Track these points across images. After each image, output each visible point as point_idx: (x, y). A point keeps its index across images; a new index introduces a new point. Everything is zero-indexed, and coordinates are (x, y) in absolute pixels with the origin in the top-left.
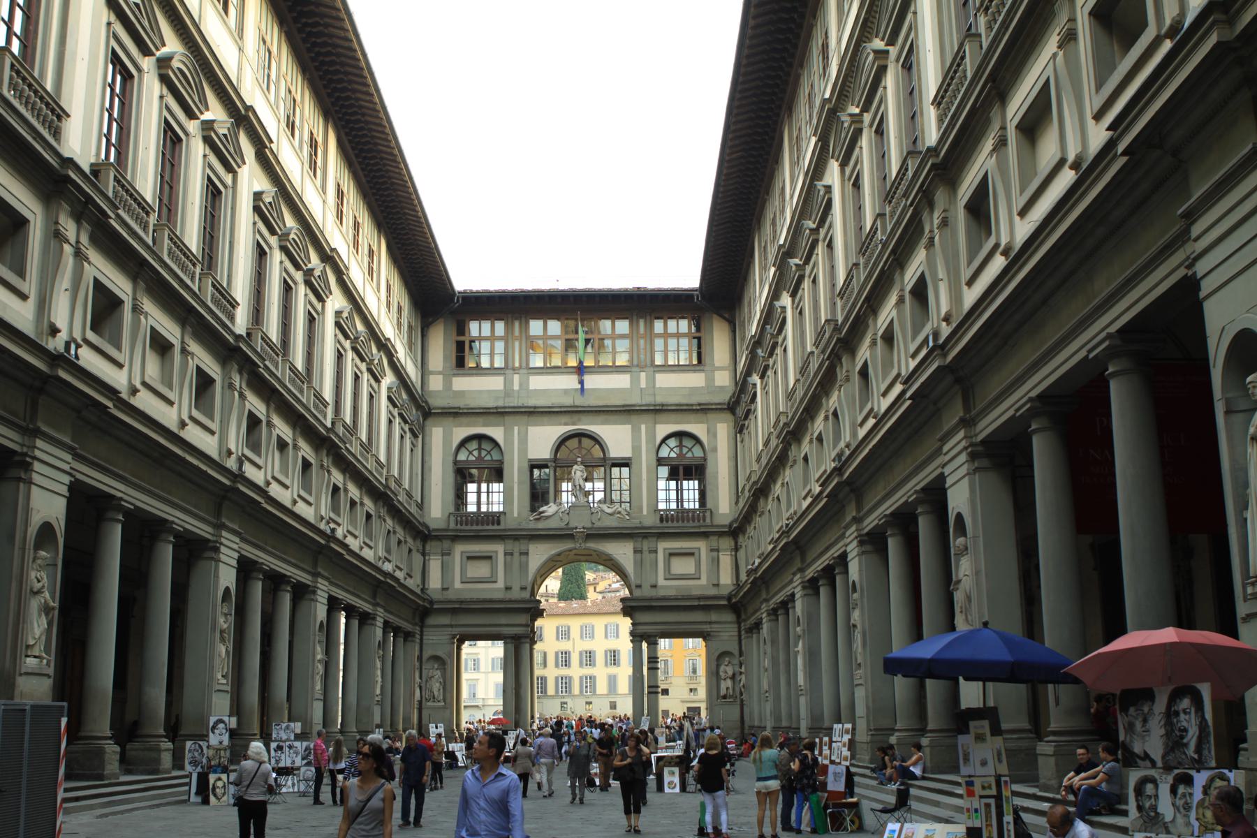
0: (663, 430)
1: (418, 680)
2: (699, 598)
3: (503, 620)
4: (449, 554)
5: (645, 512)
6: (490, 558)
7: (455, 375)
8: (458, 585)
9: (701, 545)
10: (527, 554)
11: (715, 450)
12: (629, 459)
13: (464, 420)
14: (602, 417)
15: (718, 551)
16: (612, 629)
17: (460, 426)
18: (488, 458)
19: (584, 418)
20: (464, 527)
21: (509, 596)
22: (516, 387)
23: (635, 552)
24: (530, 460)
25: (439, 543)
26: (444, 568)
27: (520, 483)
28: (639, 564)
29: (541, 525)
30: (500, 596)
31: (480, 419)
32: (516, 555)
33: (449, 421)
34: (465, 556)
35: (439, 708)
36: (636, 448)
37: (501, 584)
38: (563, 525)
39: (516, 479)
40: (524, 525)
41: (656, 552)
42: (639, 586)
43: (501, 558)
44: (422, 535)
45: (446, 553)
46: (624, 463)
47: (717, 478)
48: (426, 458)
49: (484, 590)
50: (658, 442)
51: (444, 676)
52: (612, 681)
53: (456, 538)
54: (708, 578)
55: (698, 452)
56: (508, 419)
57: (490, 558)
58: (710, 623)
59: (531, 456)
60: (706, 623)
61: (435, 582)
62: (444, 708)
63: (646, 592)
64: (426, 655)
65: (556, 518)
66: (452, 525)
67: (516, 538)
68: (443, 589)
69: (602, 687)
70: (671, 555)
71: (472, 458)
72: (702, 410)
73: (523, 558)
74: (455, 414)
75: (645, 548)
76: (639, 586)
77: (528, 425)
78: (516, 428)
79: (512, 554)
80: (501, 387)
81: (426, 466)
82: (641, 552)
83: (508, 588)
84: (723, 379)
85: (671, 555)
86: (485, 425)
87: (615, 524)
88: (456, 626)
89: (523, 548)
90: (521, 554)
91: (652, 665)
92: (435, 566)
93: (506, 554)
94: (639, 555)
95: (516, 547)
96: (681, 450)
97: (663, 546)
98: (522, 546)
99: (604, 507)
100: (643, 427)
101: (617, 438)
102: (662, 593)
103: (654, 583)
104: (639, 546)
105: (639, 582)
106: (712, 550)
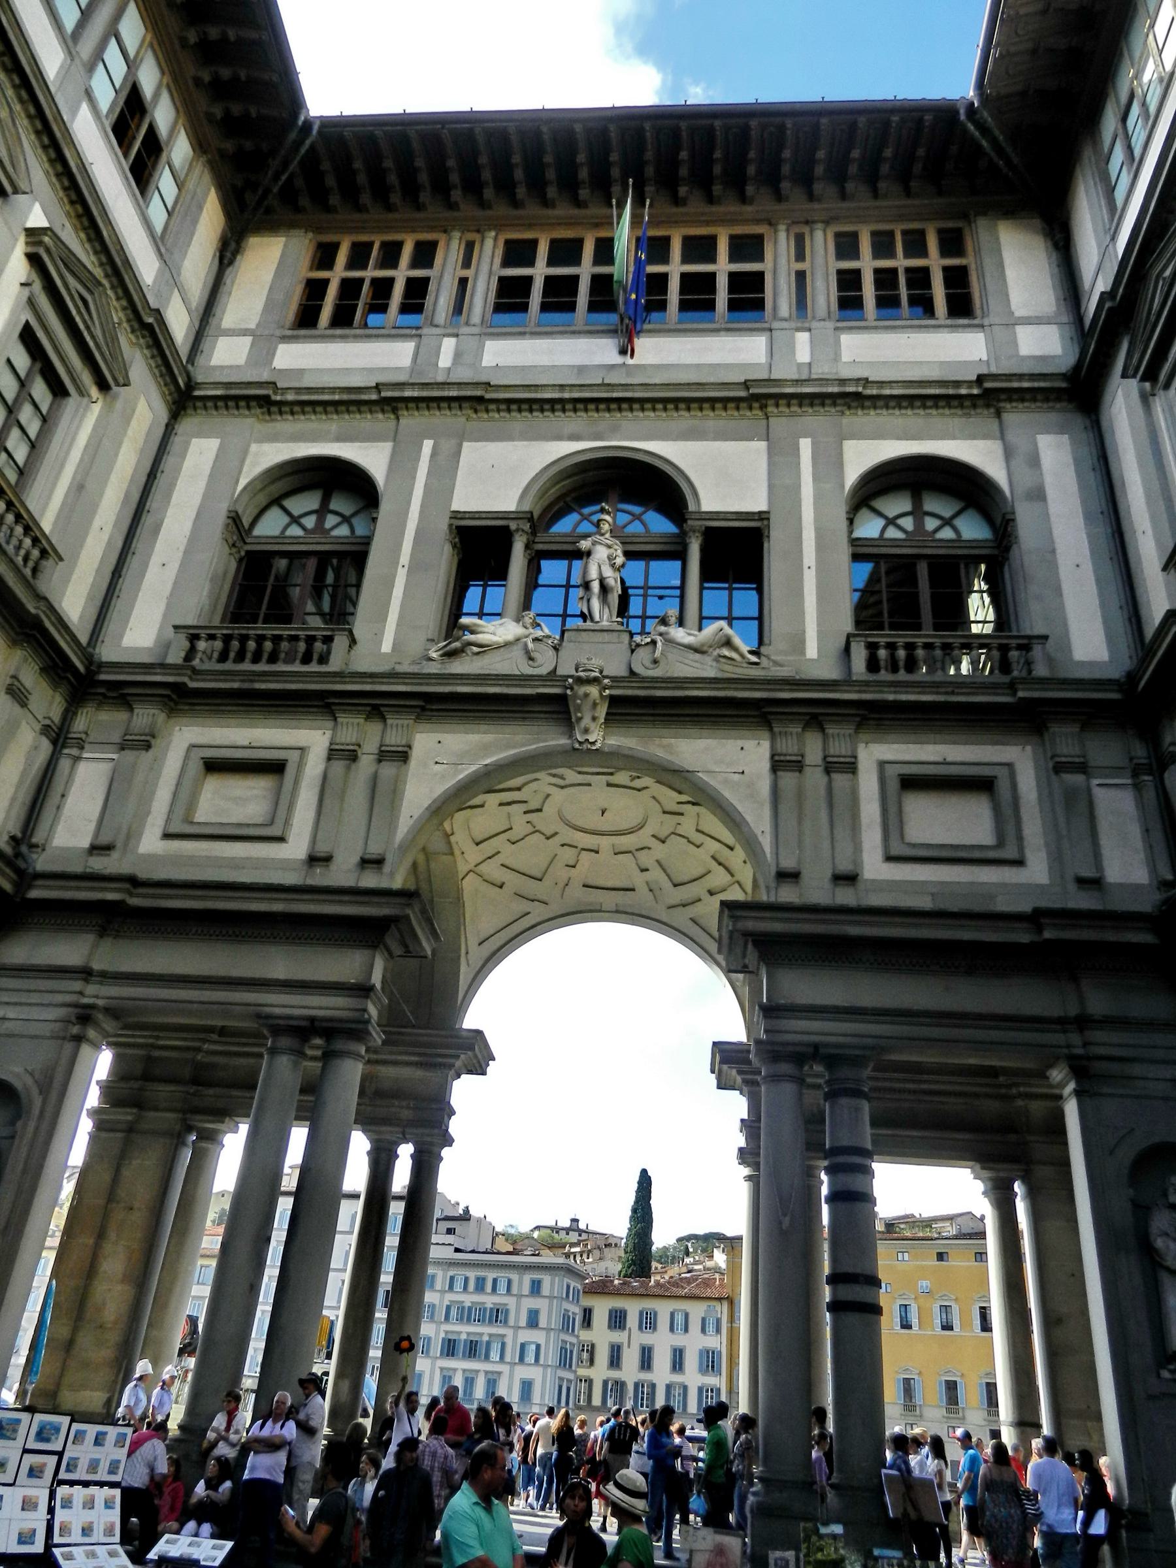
0: (864, 454)
2: (1037, 918)
3: (279, 962)
7: (285, 339)
8: (150, 842)
9: (1020, 761)
10: (402, 756)
11: (1038, 495)
12: (763, 516)
13: (287, 425)
14: (684, 420)
15: (1082, 768)
16: (679, 1318)
17: (274, 438)
19: (627, 420)
21: (320, 877)
22: (445, 361)
24: (456, 515)
25: (122, 716)
29: (458, 667)
30: (291, 878)
31: (334, 423)
32: (366, 762)
33: (245, 424)
37: (296, 848)
40: (405, 668)
41: (851, 767)
43: (315, 765)
46: (738, 553)
47: (1053, 565)
48: (153, 503)
50: (852, 474)
54: (1057, 859)
55: (972, 529)
56: (410, 421)
58: (1083, 1022)
59: (454, 507)
60: (1062, 1023)
61: (71, 830)
63: (816, 889)
68: (96, 849)
72: (987, 396)
73: (388, 770)
74: (262, 401)
76: (787, 876)
77: (462, 437)
78: (428, 446)
80: (406, 362)
81: (147, 521)
82: (798, 766)
83: (315, 860)
84: (1043, 344)
86: (340, 438)
89: (394, 739)
90: (383, 755)
93: (333, 754)
94: (788, 779)
96: (919, 524)
97: (876, 754)
98: (396, 730)
100: (805, 445)
101: (723, 474)
102: (875, 900)
103: (844, 866)
104: (788, 746)
105: (788, 864)
106: (1059, 768)
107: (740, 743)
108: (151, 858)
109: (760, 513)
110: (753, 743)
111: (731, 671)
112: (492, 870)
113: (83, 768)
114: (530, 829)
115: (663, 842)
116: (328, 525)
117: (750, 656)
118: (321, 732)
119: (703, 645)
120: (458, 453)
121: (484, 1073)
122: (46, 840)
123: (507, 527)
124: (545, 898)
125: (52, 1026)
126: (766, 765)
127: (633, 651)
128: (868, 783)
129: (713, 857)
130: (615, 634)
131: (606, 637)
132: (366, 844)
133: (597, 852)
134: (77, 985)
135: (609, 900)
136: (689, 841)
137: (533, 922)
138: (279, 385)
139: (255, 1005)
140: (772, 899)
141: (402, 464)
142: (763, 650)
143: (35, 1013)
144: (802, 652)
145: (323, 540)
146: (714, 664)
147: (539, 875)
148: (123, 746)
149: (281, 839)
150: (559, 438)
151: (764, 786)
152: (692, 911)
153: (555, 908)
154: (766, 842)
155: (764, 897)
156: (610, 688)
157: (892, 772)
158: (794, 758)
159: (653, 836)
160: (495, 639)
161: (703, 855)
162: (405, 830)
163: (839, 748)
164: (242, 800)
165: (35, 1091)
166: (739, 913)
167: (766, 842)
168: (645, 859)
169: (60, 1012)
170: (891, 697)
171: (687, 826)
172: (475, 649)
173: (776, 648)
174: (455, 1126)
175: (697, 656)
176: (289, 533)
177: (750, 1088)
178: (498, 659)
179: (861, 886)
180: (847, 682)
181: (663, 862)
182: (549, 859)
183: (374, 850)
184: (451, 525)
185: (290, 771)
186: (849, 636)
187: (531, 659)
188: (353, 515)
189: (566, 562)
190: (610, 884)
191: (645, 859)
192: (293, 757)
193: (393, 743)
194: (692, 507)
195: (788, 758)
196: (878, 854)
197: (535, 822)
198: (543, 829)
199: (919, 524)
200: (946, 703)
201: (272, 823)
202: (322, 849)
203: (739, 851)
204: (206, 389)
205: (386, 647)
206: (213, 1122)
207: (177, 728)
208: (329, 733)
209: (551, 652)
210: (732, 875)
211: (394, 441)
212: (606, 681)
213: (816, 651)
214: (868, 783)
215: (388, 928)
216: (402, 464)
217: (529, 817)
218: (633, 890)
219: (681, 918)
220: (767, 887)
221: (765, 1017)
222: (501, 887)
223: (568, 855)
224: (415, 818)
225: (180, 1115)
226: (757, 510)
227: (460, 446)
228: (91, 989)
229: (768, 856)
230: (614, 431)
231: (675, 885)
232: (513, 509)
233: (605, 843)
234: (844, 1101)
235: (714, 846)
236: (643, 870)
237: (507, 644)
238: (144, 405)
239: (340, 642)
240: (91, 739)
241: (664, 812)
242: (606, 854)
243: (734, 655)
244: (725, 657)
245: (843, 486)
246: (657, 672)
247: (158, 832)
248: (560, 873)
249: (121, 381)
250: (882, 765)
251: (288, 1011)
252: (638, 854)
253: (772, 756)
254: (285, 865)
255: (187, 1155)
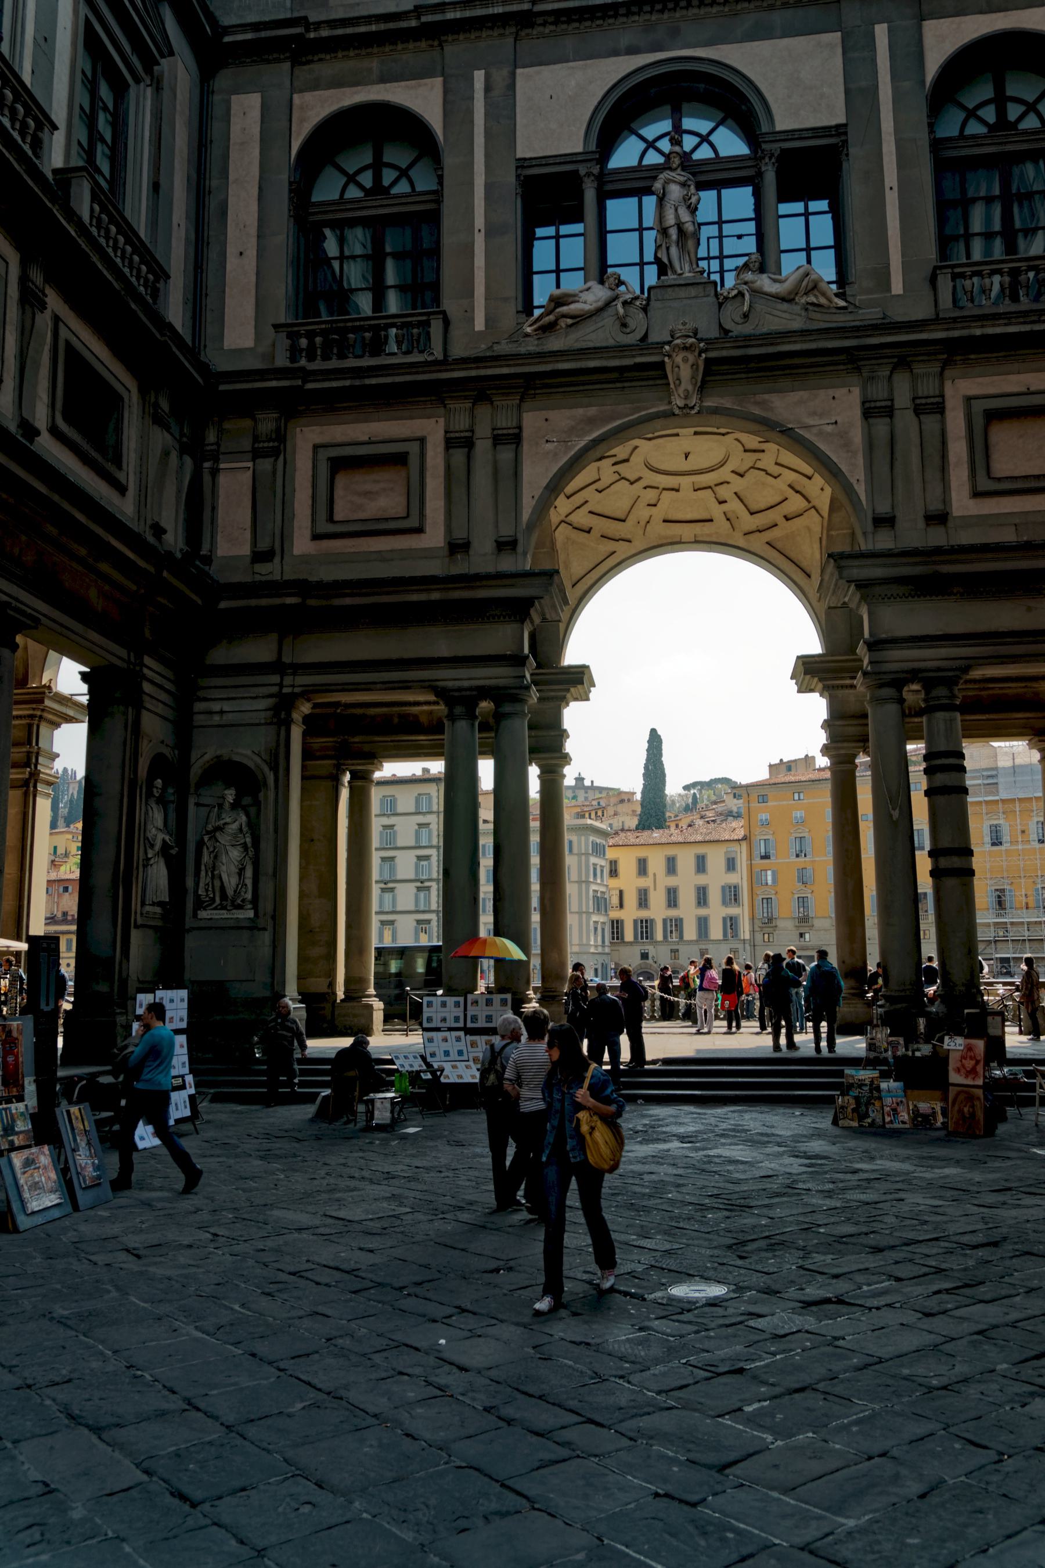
1: (158, 835)
4: (275, 453)
5: (897, 287)
6: (399, 460)
8: (302, 544)
10: (515, 439)
12: (840, 130)
13: (326, 68)
17: (315, 86)
18: (402, 187)
20: (317, 365)
23: (869, 412)
24: (522, 163)
26: (268, 500)
27: (491, 232)
28: (884, 454)
29: (555, 343)
32: (483, 446)
34: (323, 455)
35: (238, 927)
36: (859, 93)
37: (434, 537)
38: (633, 339)
39: (479, 222)
41: (940, 409)
42: (884, 522)
44: (202, 404)
45: (274, 448)
49: (382, 557)
50: (932, 68)
51: (253, 827)
52: (703, 924)
53: (298, 402)
56: (455, 50)
57: (399, 460)
61: (232, 540)
62: (253, 927)
63: (912, 533)
64: (196, 770)
65: (608, 321)
66: (282, 361)
67: (481, 391)
68: (260, 556)
69: (690, 932)
70: (993, 416)
71: (353, 193)
73: (506, 454)
75: (902, 398)
76: (884, 522)
78: (479, 76)
79: (468, 444)
81: (213, 204)
82: (889, 412)
83: (457, 547)
85: (993, 416)
86: (383, 79)
87: (797, 325)
88: (298, 668)
89: (505, 422)
91: (941, 779)
92: (233, 487)
93: (450, 443)
94: (881, 427)
95: (485, 422)
97: (963, 388)
99: (765, 283)
100: (881, 31)
102: (966, 538)
103: (935, 506)
104: (879, 392)
107: (831, 392)
108: (305, 559)
109: (838, 127)
110: (845, 390)
111: (821, 321)
112: (581, 518)
113: (223, 479)
114: (617, 477)
115: (742, 476)
116: (386, 182)
117: (836, 300)
118: (433, 420)
119: (790, 293)
120: (512, 86)
121: (588, 699)
122: (211, 551)
123: (576, 172)
124: (629, 537)
125: (263, 714)
126: (857, 412)
127: (720, 305)
128: (956, 421)
129: (790, 486)
130: (700, 287)
131: (693, 291)
132: (497, 527)
133: (677, 490)
134: (275, 679)
135: (687, 532)
136: (767, 474)
137: (618, 561)
138: (311, 20)
139: (429, 681)
140: (870, 547)
141: (456, 105)
142: (849, 290)
143: (247, 705)
144: (889, 289)
145: (385, 202)
146: (803, 313)
147: (623, 517)
148: (256, 454)
149: (420, 530)
150: (616, 53)
151: (857, 436)
152: (768, 536)
153: (638, 545)
154: (861, 490)
155: (864, 546)
156: (705, 351)
157: (978, 407)
158: (883, 404)
159: (733, 472)
160: (587, 307)
161: (781, 484)
162: (530, 511)
163: (928, 388)
164: (376, 496)
165: (266, 769)
166: (843, 563)
167: (861, 490)
168: (723, 492)
169: (270, 702)
170: (978, 332)
171: (767, 461)
172: (570, 321)
173: (860, 290)
174: (569, 747)
175: (785, 306)
176: (348, 195)
177: (829, 690)
178: (592, 328)
179: (950, 524)
180: (936, 321)
181: (739, 494)
182: (632, 502)
183: (506, 531)
184: (518, 176)
185: (414, 461)
186: (935, 268)
187: (624, 325)
188: (411, 166)
189: (636, 199)
190: (689, 517)
191: (723, 492)
192: (414, 448)
193: (504, 425)
194: (765, 129)
195: (878, 404)
196: (966, 490)
197: (620, 472)
198: (628, 477)
199: (1001, 113)
200: (1032, 332)
201: (408, 516)
202: (460, 534)
203: (818, 480)
204: (235, 33)
205: (479, 325)
206: (363, 764)
207: (298, 429)
208: (442, 420)
209: (641, 315)
210: (809, 502)
211: (443, 75)
212: (702, 345)
213: (901, 285)
214: (956, 421)
215: (532, 605)
216: (456, 105)
217: (617, 468)
218: (711, 520)
219: (757, 543)
220: (864, 534)
221: (870, 650)
222: (589, 532)
223: (651, 495)
224: (536, 498)
225: (335, 762)
226: (833, 123)
227: (513, 75)
228: (288, 680)
229: (864, 503)
230: (674, 36)
231: (752, 514)
232: (580, 149)
233: (685, 482)
234: (940, 715)
235: (791, 476)
236: (720, 503)
237: (600, 310)
238: (180, 69)
239: (436, 328)
240: (222, 450)
241: (745, 451)
242: (686, 492)
243: (823, 301)
244: (813, 304)
245: (923, 82)
246: (747, 329)
247: (308, 533)
248: (643, 512)
249: (165, 50)
250: (969, 399)
251: (458, 684)
252: (717, 489)
253: (863, 403)
254: (427, 554)
255: (345, 794)
